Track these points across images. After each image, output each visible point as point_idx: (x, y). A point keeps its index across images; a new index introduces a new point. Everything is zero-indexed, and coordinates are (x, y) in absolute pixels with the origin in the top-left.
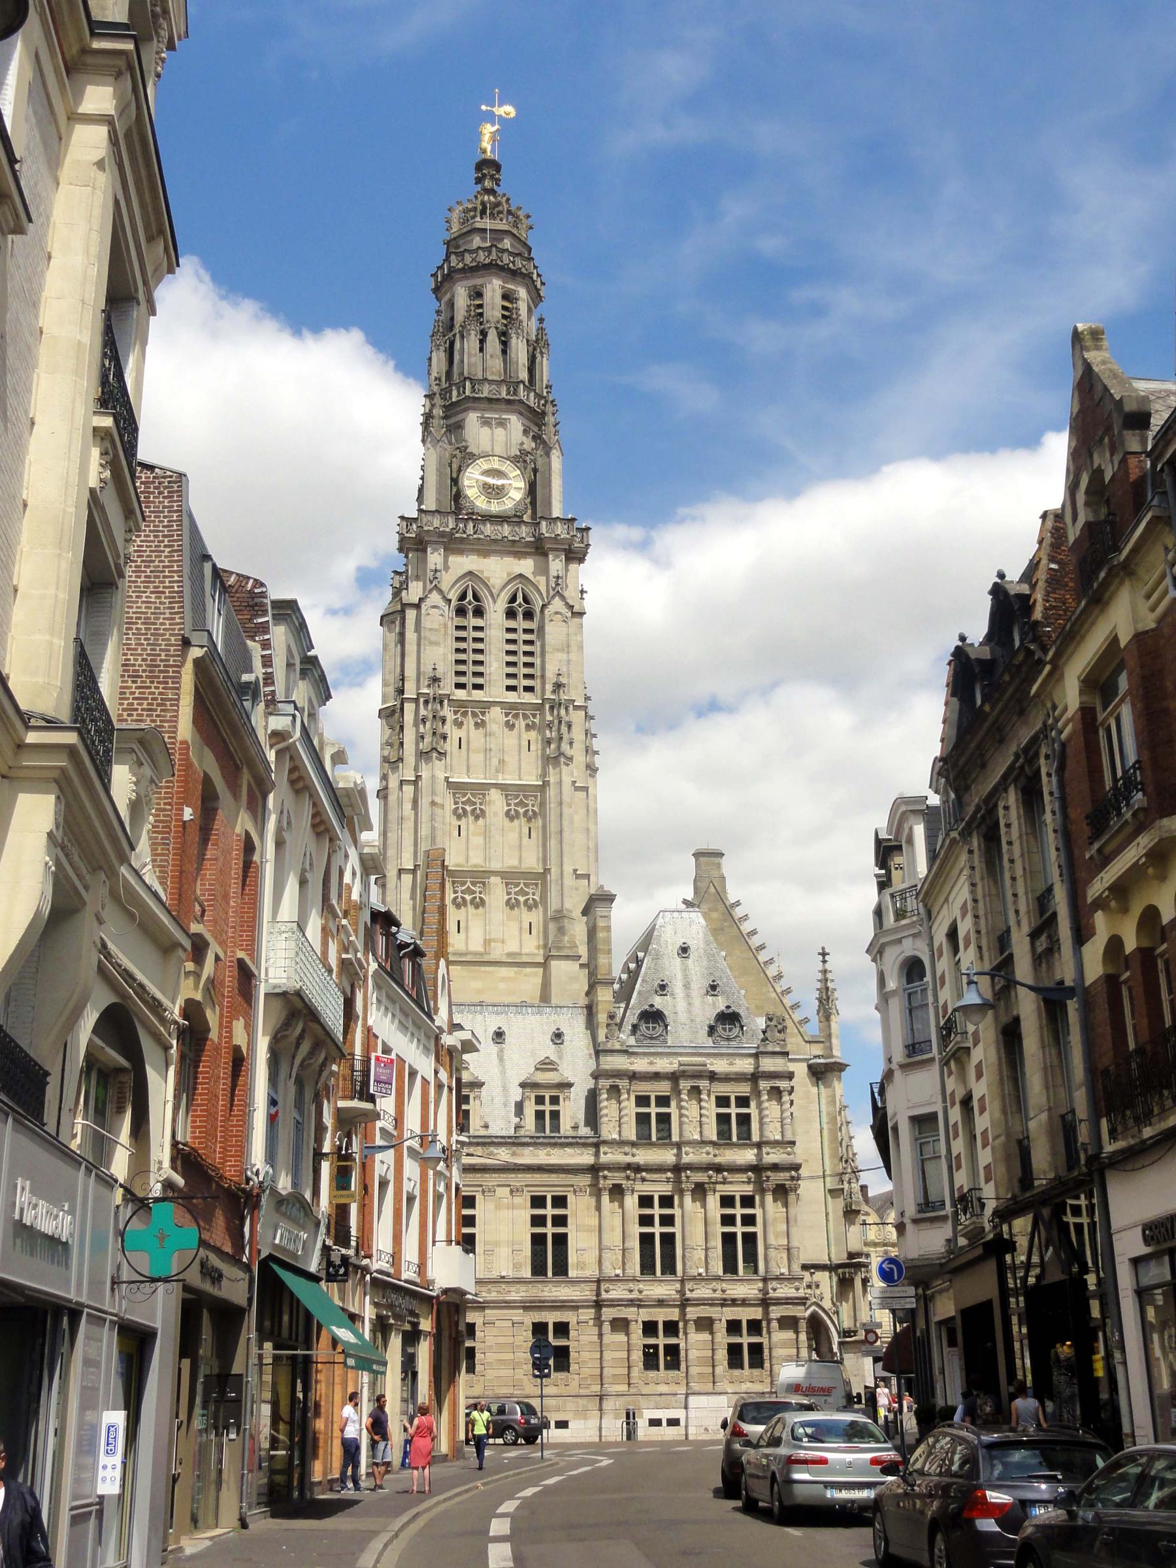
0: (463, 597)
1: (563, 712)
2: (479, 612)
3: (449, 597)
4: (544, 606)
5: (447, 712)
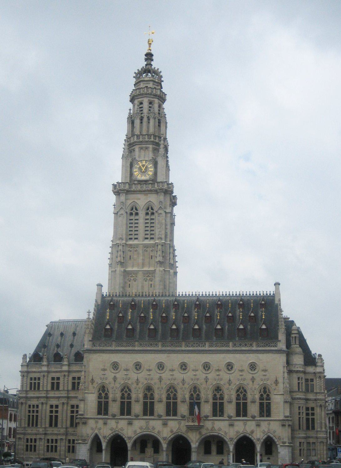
0: (132, 209)
2: (137, 214)
3: (127, 211)
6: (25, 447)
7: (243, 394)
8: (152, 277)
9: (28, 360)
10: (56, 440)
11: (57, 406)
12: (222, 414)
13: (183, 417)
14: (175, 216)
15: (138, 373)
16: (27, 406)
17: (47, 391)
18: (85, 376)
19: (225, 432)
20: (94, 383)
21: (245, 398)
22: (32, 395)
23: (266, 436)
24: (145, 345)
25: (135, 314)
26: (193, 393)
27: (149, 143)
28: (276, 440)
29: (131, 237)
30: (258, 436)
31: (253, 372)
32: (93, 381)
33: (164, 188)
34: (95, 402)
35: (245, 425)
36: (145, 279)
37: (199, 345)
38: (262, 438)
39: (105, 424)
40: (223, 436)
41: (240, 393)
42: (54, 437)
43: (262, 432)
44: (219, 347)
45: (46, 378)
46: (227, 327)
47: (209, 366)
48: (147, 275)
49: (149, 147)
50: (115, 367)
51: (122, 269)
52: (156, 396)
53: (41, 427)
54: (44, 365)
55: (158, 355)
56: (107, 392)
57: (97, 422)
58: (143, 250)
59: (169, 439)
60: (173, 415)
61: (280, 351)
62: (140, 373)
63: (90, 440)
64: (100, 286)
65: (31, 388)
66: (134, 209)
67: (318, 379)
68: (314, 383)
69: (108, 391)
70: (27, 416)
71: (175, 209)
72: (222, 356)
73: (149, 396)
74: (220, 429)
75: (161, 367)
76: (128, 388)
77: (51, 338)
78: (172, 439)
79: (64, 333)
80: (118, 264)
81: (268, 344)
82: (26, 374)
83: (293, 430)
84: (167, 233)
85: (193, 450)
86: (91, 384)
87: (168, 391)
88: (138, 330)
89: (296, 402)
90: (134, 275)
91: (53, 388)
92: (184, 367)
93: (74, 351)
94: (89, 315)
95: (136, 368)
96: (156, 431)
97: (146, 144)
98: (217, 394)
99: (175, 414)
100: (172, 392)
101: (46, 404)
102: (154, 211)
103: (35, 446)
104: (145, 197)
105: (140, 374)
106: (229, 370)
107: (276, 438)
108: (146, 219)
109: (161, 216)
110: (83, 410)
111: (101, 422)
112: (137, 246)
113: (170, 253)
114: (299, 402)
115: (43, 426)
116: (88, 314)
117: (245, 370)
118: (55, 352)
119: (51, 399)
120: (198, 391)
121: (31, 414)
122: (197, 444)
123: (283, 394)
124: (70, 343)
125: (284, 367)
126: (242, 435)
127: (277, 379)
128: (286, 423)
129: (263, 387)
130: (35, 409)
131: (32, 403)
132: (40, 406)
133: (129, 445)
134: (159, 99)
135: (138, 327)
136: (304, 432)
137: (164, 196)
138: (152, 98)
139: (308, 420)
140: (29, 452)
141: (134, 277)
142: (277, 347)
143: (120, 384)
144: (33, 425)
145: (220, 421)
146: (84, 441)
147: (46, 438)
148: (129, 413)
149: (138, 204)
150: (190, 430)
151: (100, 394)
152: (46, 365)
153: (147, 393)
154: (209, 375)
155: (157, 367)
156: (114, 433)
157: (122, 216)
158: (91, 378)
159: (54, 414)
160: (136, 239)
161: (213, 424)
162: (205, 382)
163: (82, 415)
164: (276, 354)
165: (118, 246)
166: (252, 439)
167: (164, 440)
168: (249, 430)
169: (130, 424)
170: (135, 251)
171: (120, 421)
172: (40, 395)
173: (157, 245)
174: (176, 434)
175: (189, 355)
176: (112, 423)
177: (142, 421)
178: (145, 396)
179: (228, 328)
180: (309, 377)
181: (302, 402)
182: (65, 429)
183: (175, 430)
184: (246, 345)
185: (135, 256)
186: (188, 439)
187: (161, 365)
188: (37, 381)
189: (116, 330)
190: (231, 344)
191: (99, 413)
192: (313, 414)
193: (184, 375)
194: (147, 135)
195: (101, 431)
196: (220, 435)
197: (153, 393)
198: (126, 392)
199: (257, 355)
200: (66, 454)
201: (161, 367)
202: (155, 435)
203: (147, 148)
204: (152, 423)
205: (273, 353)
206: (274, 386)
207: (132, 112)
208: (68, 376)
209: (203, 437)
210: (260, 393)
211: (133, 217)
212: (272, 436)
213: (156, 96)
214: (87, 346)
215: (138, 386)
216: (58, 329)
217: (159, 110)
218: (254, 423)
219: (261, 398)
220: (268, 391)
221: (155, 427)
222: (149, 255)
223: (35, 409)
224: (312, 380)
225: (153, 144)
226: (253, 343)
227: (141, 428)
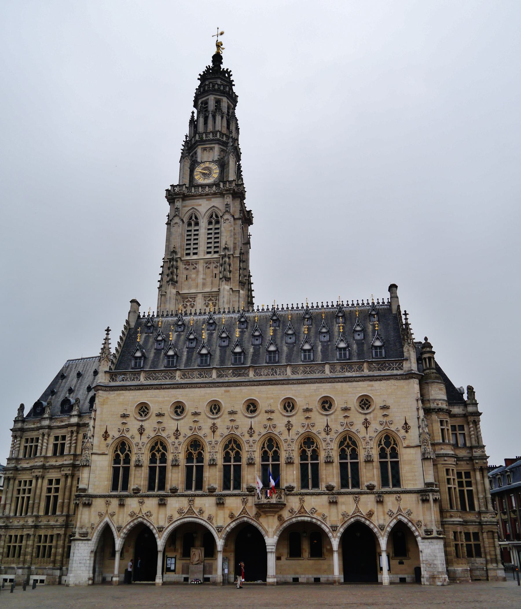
0: (191, 218)
1: (227, 259)
2: (197, 224)
4: (221, 217)
5: (181, 266)
6: (5, 550)
7: (350, 448)
8: (216, 300)
9: (26, 413)
10: (52, 536)
11: (58, 481)
12: (316, 485)
13: (251, 490)
14: (250, 235)
15: (178, 420)
16: (17, 482)
17: (46, 457)
18: (94, 427)
19: (324, 515)
20: (108, 438)
21: (355, 455)
22: (25, 465)
23: (395, 521)
24: (191, 375)
25: (182, 338)
26: (267, 450)
28: (413, 529)
29: (188, 252)
30: (381, 522)
31: (366, 412)
32: (106, 435)
33: (232, 187)
34: (107, 468)
35: (357, 501)
36: (207, 304)
37: (276, 373)
38: (388, 525)
39: (122, 505)
40: (319, 523)
41: (346, 446)
42: (49, 533)
43: (388, 514)
44: (308, 373)
45: (46, 437)
46: (320, 348)
47: (292, 404)
48: (209, 299)
50: (144, 411)
51: (174, 291)
52: (207, 457)
53: (31, 516)
54: (45, 418)
55: (212, 389)
56: (129, 453)
57: (108, 504)
58: (203, 266)
59: (228, 529)
60: (235, 488)
61: (409, 376)
62: (182, 419)
63: (95, 534)
64: (135, 302)
65: (25, 456)
66: (193, 218)
67: (472, 425)
68: (466, 431)
69: (130, 451)
70: (14, 499)
71: (251, 229)
72: (313, 387)
73: (195, 456)
74: (314, 511)
75: (215, 408)
76: (162, 444)
77: (64, 381)
78: (233, 530)
80: (169, 285)
81: (387, 365)
82: (19, 433)
83: (442, 512)
84: (236, 244)
85: (269, 548)
86: (103, 439)
87: (226, 447)
88: (184, 358)
89: (441, 461)
90: (191, 300)
91: (55, 453)
92: (252, 408)
93: (91, 394)
94: (108, 334)
95: (176, 412)
96: (205, 516)
97: (211, 144)
98: (307, 449)
99: (238, 486)
100: (232, 449)
101: (43, 478)
102: (220, 219)
103: (20, 547)
104: (208, 202)
105: (182, 421)
106: (326, 410)
107: (413, 524)
108: (209, 229)
109: (227, 222)
110: (86, 482)
111: (115, 502)
112: (196, 262)
113: (240, 269)
114: (445, 460)
115: (35, 513)
116: (106, 332)
117: (353, 408)
119: (50, 471)
120: (275, 445)
121: (21, 495)
122: (276, 538)
123: (420, 446)
124: (87, 386)
125: (417, 400)
126: (352, 520)
127: (407, 422)
128: (429, 495)
129: (384, 436)
131: (24, 477)
133: (161, 543)
134: (228, 98)
135: (185, 353)
136: (459, 514)
137: (233, 200)
138: (219, 95)
139: (462, 492)
140: (10, 558)
141: (191, 302)
142: (402, 370)
143: (148, 438)
144: (21, 514)
145: (315, 496)
146: (85, 536)
147: (37, 534)
148: (162, 487)
149: (198, 211)
150: (263, 512)
151: (117, 456)
152: (47, 418)
153: (193, 452)
154: (294, 418)
155: (208, 409)
156: (135, 521)
157: (177, 225)
158: (105, 430)
159: (52, 494)
161: (302, 501)
162: (287, 431)
163: (84, 490)
164: (402, 381)
165: (170, 262)
166: (372, 526)
167: (219, 532)
168: (364, 511)
169: (162, 504)
171: (146, 500)
172: (35, 464)
173: (222, 258)
174: (238, 521)
175: (260, 387)
176: (133, 504)
177: (183, 499)
178: (189, 458)
179: (321, 350)
180: (458, 422)
181: (452, 461)
182: (65, 518)
183: (237, 514)
184: (351, 368)
185: (194, 276)
186: (260, 528)
187: (215, 405)
189: (151, 358)
190: (327, 367)
191: (115, 487)
192: (469, 484)
193: (253, 420)
194: (211, 134)
195: (115, 518)
196: (314, 520)
197: (202, 451)
198: (158, 451)
200: (65, 560)
201: (215, 408)
202: (204, 523)
203: (211, 149)
204: (199, 502)
205: (397, 379)
206: (402, 433)
207: (195, 115)
208: (78, 433)
209: (285, 525)
210: (379, 446)
211: (193, 228)
212: (406, 521)
214: (102, 379)
215: (177, 441)
217: (228, 112)
218: (371, 498)
219: (382, 454)
220: (392, 442)
221: (204, 509)
222: (212, 272)
223: (27, 487)
224: (462, 428)
225: (218, 144)
226: (363, 365)
227: (180, 512)
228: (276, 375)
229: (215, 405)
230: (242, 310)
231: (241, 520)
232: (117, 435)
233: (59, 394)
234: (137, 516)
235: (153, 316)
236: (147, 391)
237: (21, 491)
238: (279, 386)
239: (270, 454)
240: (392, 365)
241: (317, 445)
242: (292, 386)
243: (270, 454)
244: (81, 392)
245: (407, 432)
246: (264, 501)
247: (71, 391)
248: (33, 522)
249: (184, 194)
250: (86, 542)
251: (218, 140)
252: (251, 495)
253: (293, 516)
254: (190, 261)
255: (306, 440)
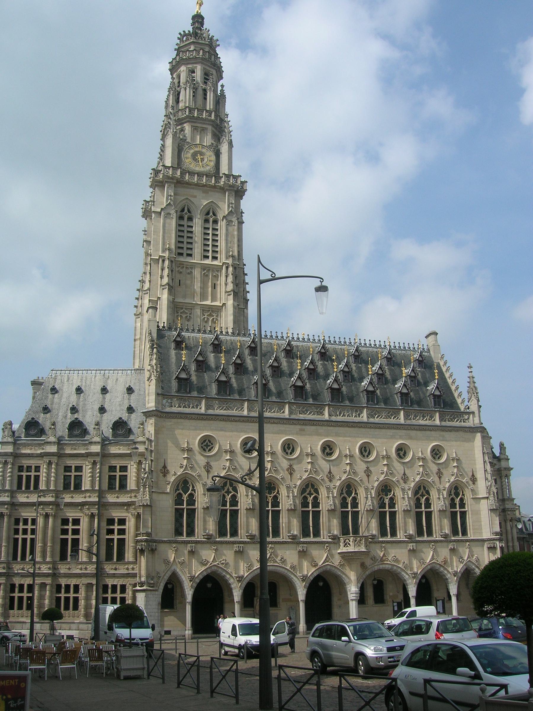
2: (190, 219)
16: (13, 520)
27: (208, 122)
42: (73, 582)
49: (207, 129)
53: (44, 562)
54: (50, 443)
55: (285, 426)
65: (19, 486)
66: (186, 211)
77: (56, 395)
79: (83, 388)
80: (163, 289)
87: (303, 491)
92: (328, 450)
97: (204, 123)
104: (204, 195)
118: (69, 421)
121: (20, 536)
123: (487, 498)
124: (97, 407)
127: (475, 474)
129: (454, 486)
130: (29, 527)
132: (40, 521)
140: (15, 611)
141: (186, 313)
145: (394, 544)
152: (54, 443)
160: (190, 255)
164: (469, 433)
168: (440, 560)
170: (189, 273)
175: (337, 428)
186: (344, 576)
188: (33, 474)
191: (178, 532)
196: (395, 568)
199: (442, 433)
205: (465, 431)
209: (367, 573)
211: (185, 222)
213: (214, 66)
216: (68, 381)
220: (461, 494)
223: (29, 527)
226: (435, 414)
228: (353, 416)
229: (289, 445)
230: (253, 334)
231: (324, 568)
232: (180, 472)
233: (54, 412)
234: (211, 564)
235: (164, 327)
236: (212, 422)
237: (21, 531)
238: (356, 429)
239: (349, 500)
240: (459, 416)
241: (394, 493)
242: (369, 430)
243: (349, 500)
244: (89, 413)
245: (474, 484)
246: (351, 549)
247: (74, 410)
248: (49, 568)
249: (177, 179)
250: (154, 592)
251: (213, 121)
252: (334, 543)
253: (377, 564)
254: (185, 263)
255: (383, 488)
